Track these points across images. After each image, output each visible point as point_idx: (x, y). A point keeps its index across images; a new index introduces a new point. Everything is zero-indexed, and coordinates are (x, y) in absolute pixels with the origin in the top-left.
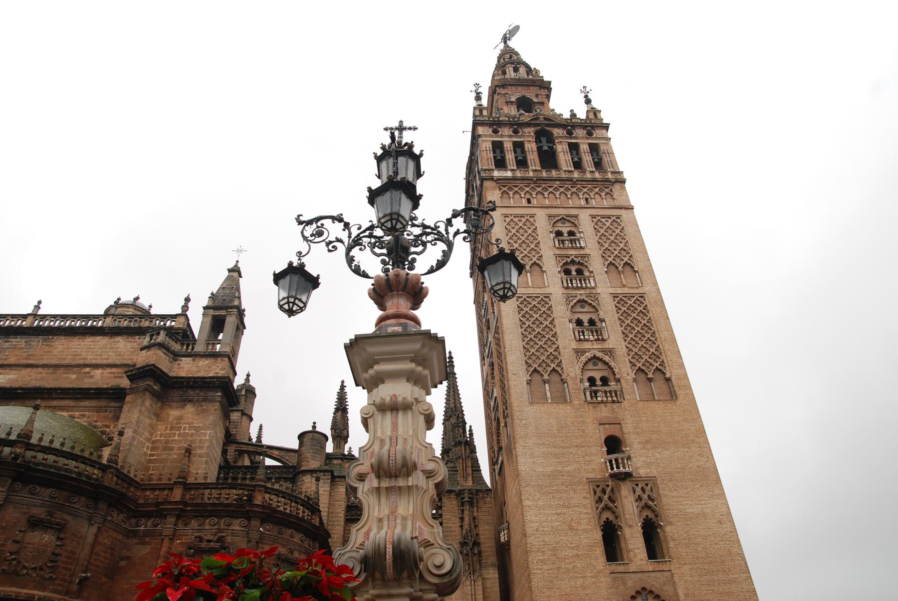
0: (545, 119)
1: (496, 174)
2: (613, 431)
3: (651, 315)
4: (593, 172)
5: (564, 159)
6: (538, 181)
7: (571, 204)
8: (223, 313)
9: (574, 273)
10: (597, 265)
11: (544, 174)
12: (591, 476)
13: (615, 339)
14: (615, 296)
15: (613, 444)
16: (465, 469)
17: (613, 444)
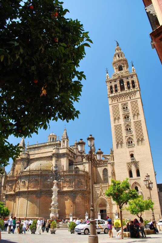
0: (121, 76)
1: (111, 95)
2: (131, 153)
3: (142, 125)
4: (132, 89)
5: (126, 86)
6: (120, 96)
7: (127, 100)
8: (64, 140)
9: (127, 118)
10: (131, 116)
11: (121, 93)
12: (127, 162)
13: (134, 133)
14: (134, 122)
15: (132, 156)
16: (112, 158)
17: (132, 156)
